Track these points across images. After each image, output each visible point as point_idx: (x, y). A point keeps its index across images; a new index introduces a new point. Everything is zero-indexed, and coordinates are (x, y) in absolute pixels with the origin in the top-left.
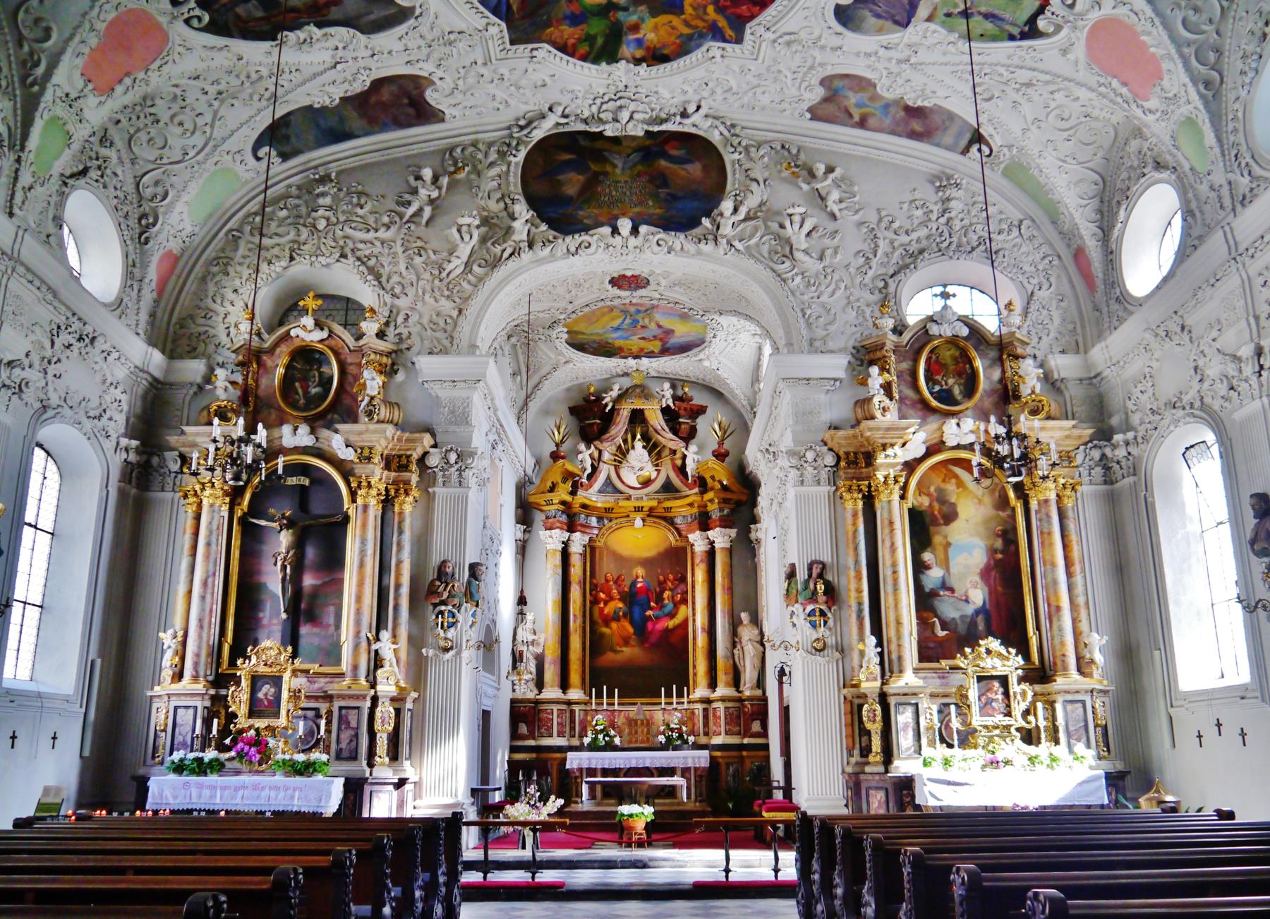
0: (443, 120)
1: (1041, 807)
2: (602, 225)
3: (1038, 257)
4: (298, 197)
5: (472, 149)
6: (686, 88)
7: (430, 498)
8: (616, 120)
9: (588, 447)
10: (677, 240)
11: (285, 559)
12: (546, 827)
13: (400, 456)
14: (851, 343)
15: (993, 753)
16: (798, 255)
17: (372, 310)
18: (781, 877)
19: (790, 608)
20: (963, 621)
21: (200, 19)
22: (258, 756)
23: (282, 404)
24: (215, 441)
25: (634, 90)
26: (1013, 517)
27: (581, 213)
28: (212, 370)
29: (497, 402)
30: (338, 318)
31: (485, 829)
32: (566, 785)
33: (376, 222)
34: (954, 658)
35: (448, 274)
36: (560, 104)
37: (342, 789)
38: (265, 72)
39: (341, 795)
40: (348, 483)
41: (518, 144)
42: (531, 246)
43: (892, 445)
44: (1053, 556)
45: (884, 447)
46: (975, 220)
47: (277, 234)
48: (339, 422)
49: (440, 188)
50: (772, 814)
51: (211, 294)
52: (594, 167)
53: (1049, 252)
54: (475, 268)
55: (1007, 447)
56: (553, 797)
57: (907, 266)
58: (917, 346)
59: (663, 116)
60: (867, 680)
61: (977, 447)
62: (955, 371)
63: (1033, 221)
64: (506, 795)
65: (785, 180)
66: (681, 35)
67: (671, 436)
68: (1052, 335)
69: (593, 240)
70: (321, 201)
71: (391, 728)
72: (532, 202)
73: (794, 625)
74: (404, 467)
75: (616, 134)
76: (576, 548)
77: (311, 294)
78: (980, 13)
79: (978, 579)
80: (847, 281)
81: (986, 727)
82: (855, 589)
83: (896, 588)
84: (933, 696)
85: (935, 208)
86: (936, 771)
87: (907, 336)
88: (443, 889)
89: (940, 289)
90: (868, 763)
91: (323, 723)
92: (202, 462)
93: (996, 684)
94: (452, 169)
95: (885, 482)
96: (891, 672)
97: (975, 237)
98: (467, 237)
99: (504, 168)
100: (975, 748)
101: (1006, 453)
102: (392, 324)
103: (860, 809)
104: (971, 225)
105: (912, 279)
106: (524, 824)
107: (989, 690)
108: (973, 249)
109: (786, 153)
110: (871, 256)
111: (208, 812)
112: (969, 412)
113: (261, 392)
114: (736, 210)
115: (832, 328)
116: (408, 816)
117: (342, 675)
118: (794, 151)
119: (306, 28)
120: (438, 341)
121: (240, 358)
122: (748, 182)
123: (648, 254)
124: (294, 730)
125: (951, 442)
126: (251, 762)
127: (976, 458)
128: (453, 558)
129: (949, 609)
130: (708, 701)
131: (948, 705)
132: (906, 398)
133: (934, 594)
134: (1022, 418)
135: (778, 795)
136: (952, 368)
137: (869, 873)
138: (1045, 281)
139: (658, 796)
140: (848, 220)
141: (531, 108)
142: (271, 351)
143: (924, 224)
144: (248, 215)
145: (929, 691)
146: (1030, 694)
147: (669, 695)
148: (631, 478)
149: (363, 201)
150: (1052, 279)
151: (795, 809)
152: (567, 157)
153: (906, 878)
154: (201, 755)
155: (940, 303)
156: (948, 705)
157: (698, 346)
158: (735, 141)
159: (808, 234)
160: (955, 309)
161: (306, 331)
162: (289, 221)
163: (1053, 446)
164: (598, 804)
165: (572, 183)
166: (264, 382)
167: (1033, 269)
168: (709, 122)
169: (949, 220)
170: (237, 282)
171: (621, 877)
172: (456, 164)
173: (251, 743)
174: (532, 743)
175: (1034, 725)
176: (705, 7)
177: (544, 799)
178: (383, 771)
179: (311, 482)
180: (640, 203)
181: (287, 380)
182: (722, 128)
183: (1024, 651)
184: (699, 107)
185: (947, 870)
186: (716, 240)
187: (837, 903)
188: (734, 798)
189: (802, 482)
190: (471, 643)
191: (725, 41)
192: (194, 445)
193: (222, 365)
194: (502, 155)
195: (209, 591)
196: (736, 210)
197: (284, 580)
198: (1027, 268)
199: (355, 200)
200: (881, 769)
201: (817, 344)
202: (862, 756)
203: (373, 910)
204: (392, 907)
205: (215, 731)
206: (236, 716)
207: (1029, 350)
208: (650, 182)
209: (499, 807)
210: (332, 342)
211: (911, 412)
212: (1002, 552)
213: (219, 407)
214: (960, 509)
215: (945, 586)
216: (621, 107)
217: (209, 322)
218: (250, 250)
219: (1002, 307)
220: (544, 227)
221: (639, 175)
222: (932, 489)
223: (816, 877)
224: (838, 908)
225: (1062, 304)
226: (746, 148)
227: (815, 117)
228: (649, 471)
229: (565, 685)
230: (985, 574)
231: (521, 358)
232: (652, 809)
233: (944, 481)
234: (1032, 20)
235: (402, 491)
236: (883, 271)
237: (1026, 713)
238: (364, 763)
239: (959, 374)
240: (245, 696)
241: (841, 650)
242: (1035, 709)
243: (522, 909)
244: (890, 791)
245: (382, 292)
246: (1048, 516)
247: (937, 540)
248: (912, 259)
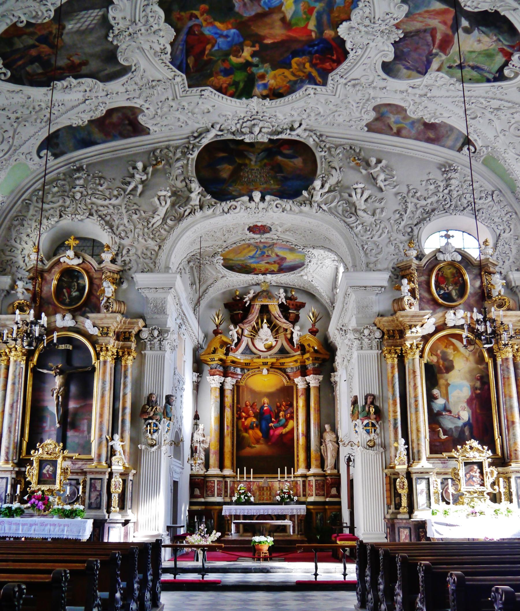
0: (149, 134)
1: (501, 539)
2: (243, 195)
3: (504, 213)
4: (64, 180)
5: (166, 150)
6: (293, 113)
7: (142, 357)
8: (251, 133)
9: (235, 327)
10: (288, 204)
11: (58, 392)
12: (209, 549)
13: (125, 332)
14: (391, 265)
15: (473, 507)
16: (360, 213)
17: (108, 247)
18: (348, 578)
19: (354, 422)
21: (5, 74)
22: (43, 507)
23: (56, 303)
24: (17, 323)
25: (262, 115)
26: (487, 368)
27: (231, 188)
28: (14, 282)
29: (182, 300)
30: (88, 252)
31: (175, 550)
32: (222, 524)
33: (110, 194)
34: (451, 451)
35: (153, 225)
36: (218, 123)
37: (92, 526)
38: (44, 106)
39: (91, 529)
40: (95, 348)
41: (193, 148)
42: (201, 208)
43: (415, 326)
44: (510, 392)
45: (410, 327)
46: (466, 191)
47: (52, 202)
48: (89, 313)
49: (147, 174)
50: (342, 542)
51: (14, 237)
52: (239, 161)
53: (510, 210)
54: (169, 221)
55: (483, 327)
56: (214, 532)
57: (425, 219)
58: (430, 266)
59: (280, 130)
60: (399, 464)
61: (466, 327)
62: (453, 281)
63: (501, 191)
64: (187, 530)
65: (352, 168)
68: (511, 260)
69: (238, 204)
70: (78, 182)
71: (120, 491)
72: (202, 182)
73: (357, 432)
74: (127, 339)
75: (252, 141)
77: (72, 237)
78: (469, 66)
79: (465, 405)
80: (389, 228)
81: (469, 492)
82: (393, 411)
83: (417, 411)
84: (438, 474)
85: (442, 184)
86: (440, 517)
87: (424, 261)
88: (151, 584)
89: (445, 233)
90: (399, 513)
91: (81, 487)
92: (10, 336)
93: (476, 467)
94: (154, 162)
95: (411, 348)
96: (414, 459)
97: (466, 202)
98: (163, 203)
99: (185, 162)
100: (463, 504)
101: (483, 330)
102: (120, 255)
103: (395, 540)
104: (463, 194)
105: (427, 227)
106: (198, 547)
107: (471, 470)
108: (464, 208)
109: (353, 152)
110: (403, 213)
111: (15, 538)
112: (461, 306)
113: (44, 295)
114: (323, 186)
115: (380, 256)
116: (131, 541)
117: (92, 460)
118: (358, 151)
119: (68, 79)
120: (147, 264)
121: (31, 275)
122: (330, 169)
123: (271, 213)
124: (64, 491)
125: (450, 324)
126: (39, 510)
127: (465, 334)
128: (156, 392)
129: (448, 423)
130: (305, 476)
131: (447, 479)
132: (424, 298)
133: (439, 414)
134: (493, 309)
135: (347, 531)
136: (451, 280)
137: (399, 576)
138: (507, 228)
139: (276, 531)
140: (390, 191)
141: (201, 126)
142: (49, 270)
143: (435, 194)
144: (35, 190)
145: (436, 471)
146: (495, 473)
147: (282, 472)
149: (102, 182)
150: (512, 227)
151: (356, 539)
152: (222, 155)
153: (420, 579)
154: (10, 505)
155: (444, 241)
156: (447, 479)
157: (300, 267)
158: (322, 145)
159: (366, 200)
160: (453, 245)
161: (69, 259)
162: (59, 194)
163: (511, 326)
164: (241, 536)
165: (225, 170)
166: (45, 289)
167: (500, 220)
168: (307, 133)
169: (450, 191)
170: (29, 230)
171: (254, 578)
172: (157, 159)
173: (39, 499)
175: (497, 491)
177: (209, 532)
178: (116, 516)
179: (73, 348)
180: (266, 182)
181: (59, 288)
182: (314, 137)
183: (492, 447)
184: (301, 125)
185: (445, 575)
186: (311, 204)
187: (380, 594)
188: (321, 532)
189: (362, 348)
190: (166, 442)
192: (5, 326)
193: (21, 279)
194: (184, 154)
195: (14, 411)
196: (323, 186)
197: (58, 404)
198: (496, 220)
199: (97, 181)
200: (407, 516)
201: (371, 266)
202: (396, 508)
203: (110, 594)
204: (121, 593)
205: (18, 492)
206: (30, 483)
207: (497, 269)
208: (272, 169)
209: (184, 537)
210: (84, 265)
211: (427, 306)
212: (479, 390)
213: (19, 303)
214: (455, 364)
215: (446, 409)
216: (254, 125)
217: (13, 254)
218: (36, 211)
219: (481, 243)
220: (209, 197)
221: (265, 165)
222: (439, 352)
223: (368, 578)
224: (380, 597)
225: (517, 241)
226: (329, 149)
227: (370, 130)
229: (221, 467)
230: (470, 402)
231: (196, 274)
232: (272, 539)
233: (446, 347)
234: (501, 70)
235: (126, 353)
236: (410, 222)
237: (493, 484)
238: (105, 511)
239: (455, 283)
240: (35, 472)
241: (384, 446)
242: (498, 482)
243: (196, 596)
244: (412, 529)
245: (114, 236)
246: (508, 368)
247: (442, 382)
248: (428, 215)
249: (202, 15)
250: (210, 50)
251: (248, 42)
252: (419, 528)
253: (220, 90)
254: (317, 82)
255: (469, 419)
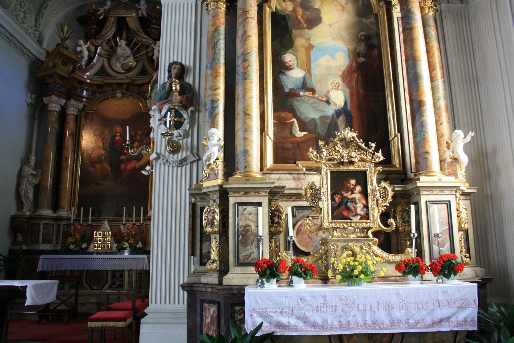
20: (322, 122)
67: (143, 35)
76: (72, 111)
79: (339, 80)
129: (309, 110)
133: (293, 94)
146: (390, 194)
148: (118, 67)
174: (24, 247)
214: (322, 15)
215: (305, 86)
228: (131, 61)
230: (347, 76)
247: (299, 42)
252: (233, 305)
255: (346, 104)
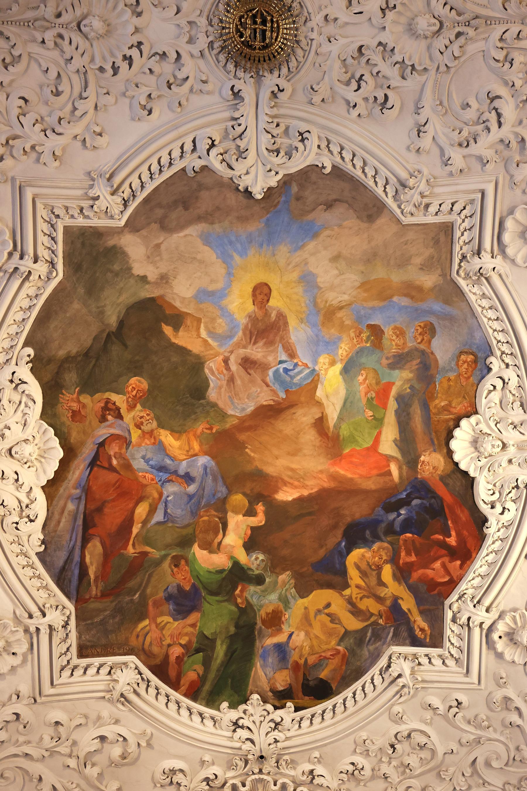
66: (347, 633)
176: (379, 569)
191: (415, 642)
249: (131, 407)
250: (145, 522)
251: (238, 499)
253: (163, 670)
254: (418, 632)
